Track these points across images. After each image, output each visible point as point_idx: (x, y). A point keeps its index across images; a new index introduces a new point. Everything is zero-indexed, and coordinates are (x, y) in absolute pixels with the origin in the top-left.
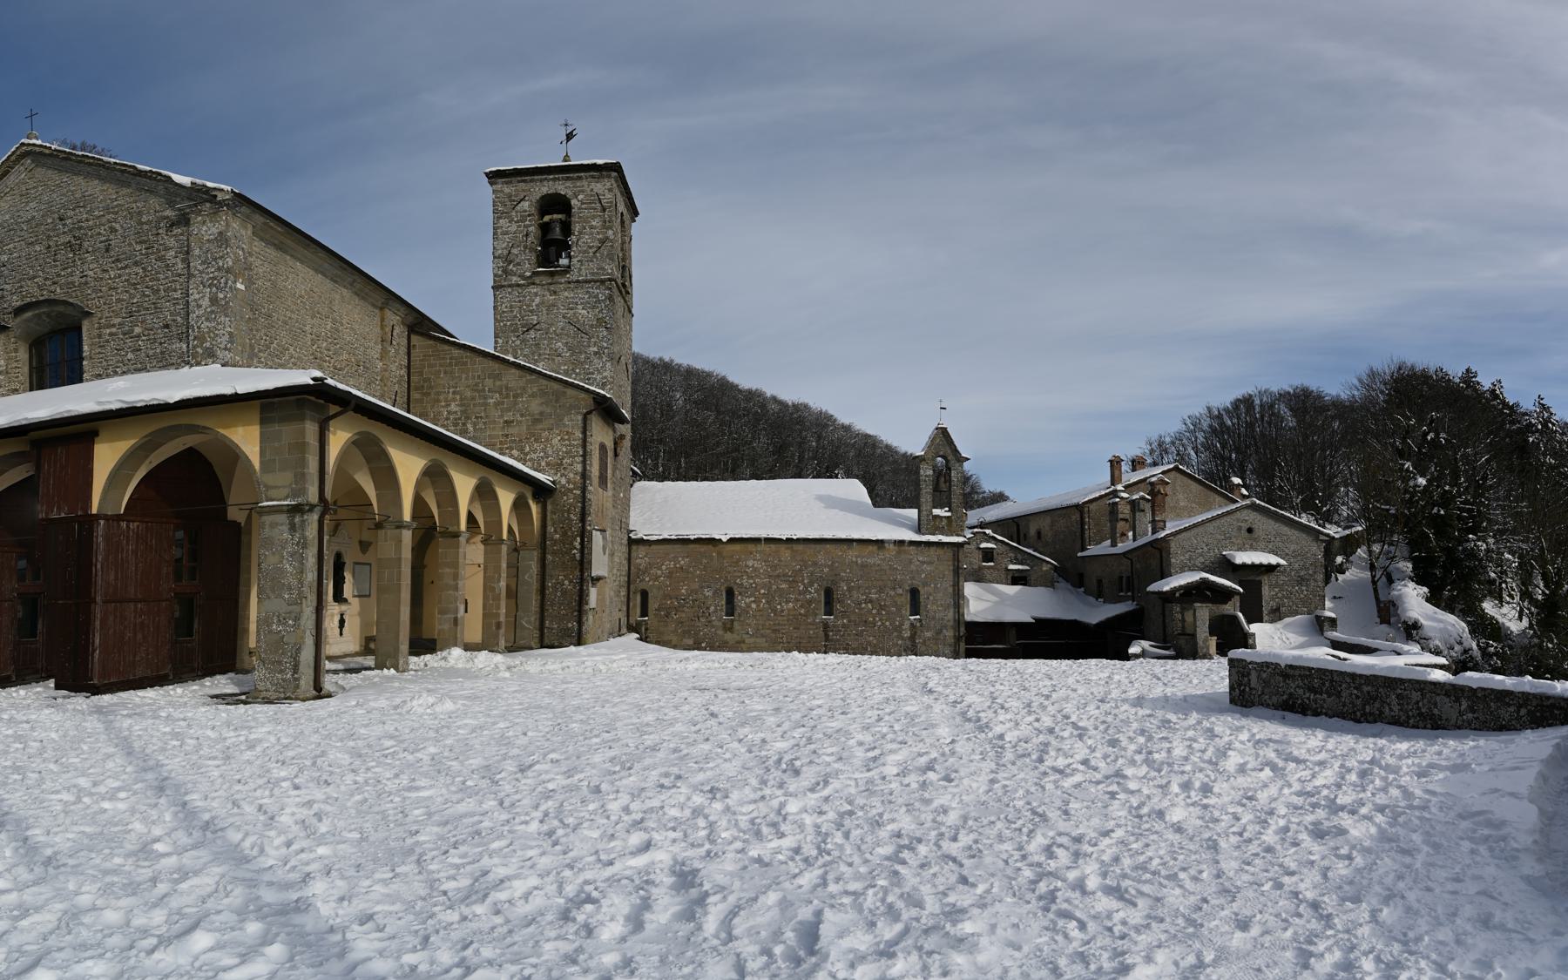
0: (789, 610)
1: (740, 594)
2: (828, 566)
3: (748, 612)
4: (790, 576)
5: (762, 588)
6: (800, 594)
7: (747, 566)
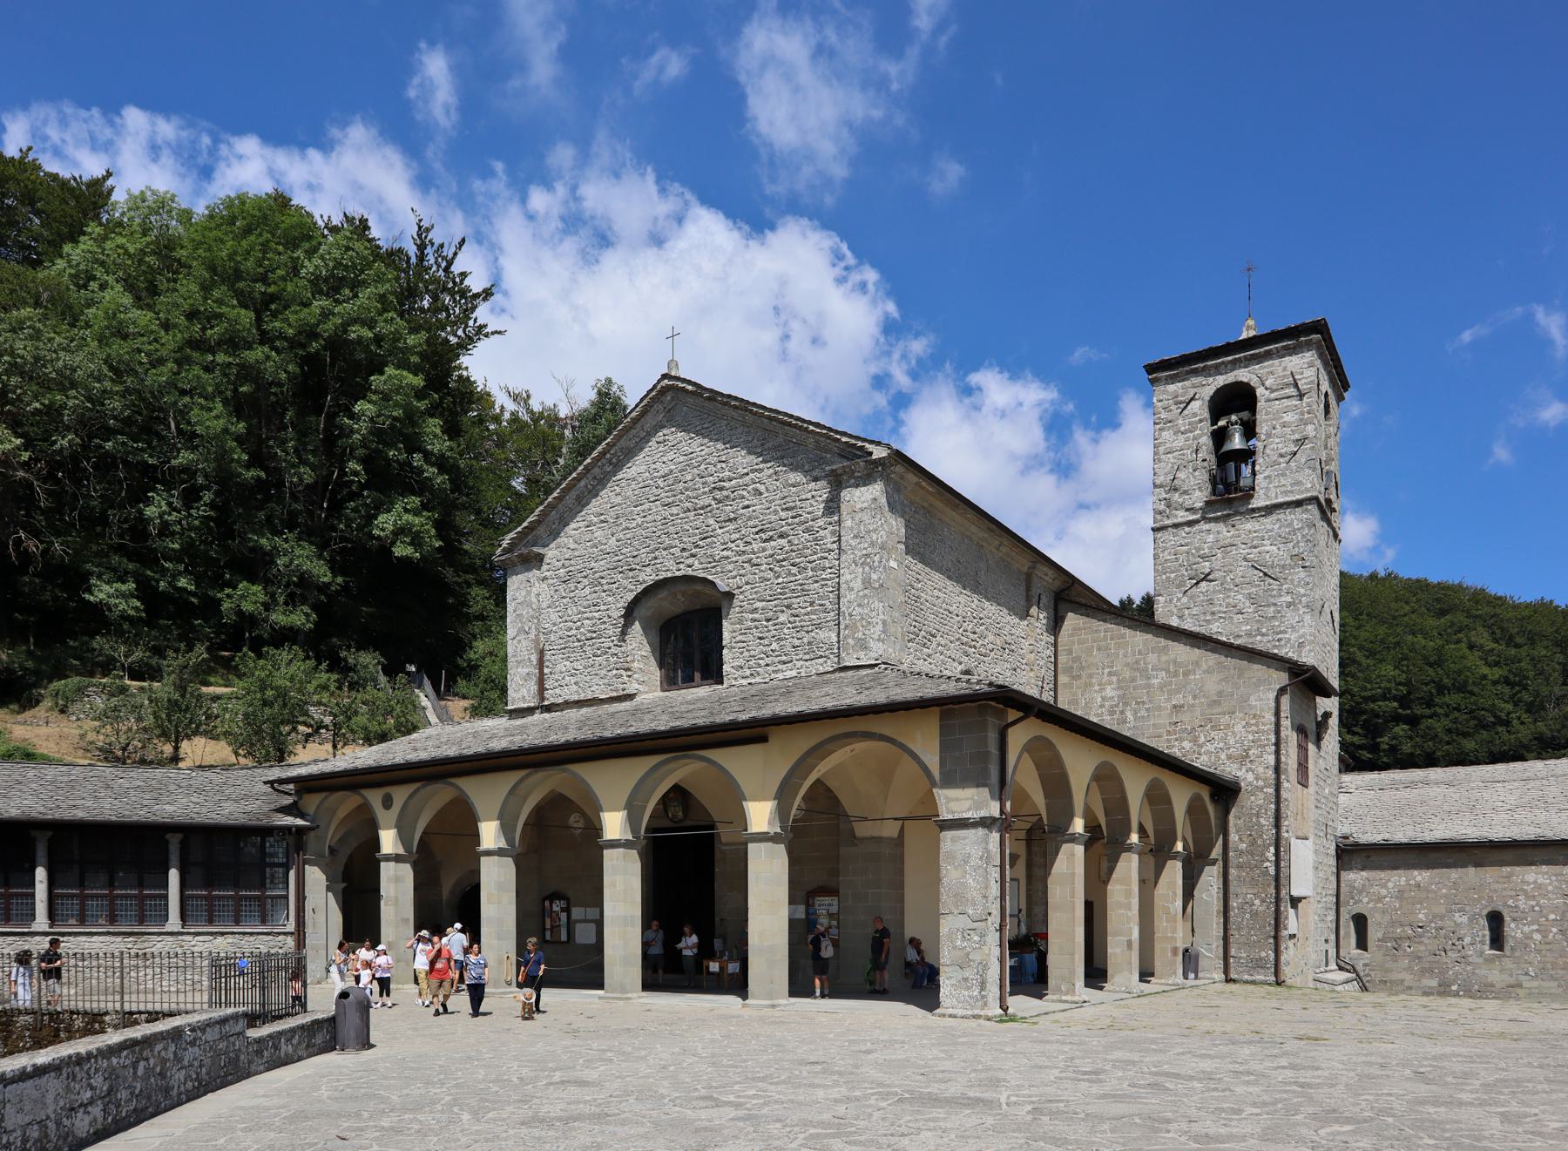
1: (1514, 920)
3: (1526, 946)
5: (1553, 912)
7: (1528, 883)
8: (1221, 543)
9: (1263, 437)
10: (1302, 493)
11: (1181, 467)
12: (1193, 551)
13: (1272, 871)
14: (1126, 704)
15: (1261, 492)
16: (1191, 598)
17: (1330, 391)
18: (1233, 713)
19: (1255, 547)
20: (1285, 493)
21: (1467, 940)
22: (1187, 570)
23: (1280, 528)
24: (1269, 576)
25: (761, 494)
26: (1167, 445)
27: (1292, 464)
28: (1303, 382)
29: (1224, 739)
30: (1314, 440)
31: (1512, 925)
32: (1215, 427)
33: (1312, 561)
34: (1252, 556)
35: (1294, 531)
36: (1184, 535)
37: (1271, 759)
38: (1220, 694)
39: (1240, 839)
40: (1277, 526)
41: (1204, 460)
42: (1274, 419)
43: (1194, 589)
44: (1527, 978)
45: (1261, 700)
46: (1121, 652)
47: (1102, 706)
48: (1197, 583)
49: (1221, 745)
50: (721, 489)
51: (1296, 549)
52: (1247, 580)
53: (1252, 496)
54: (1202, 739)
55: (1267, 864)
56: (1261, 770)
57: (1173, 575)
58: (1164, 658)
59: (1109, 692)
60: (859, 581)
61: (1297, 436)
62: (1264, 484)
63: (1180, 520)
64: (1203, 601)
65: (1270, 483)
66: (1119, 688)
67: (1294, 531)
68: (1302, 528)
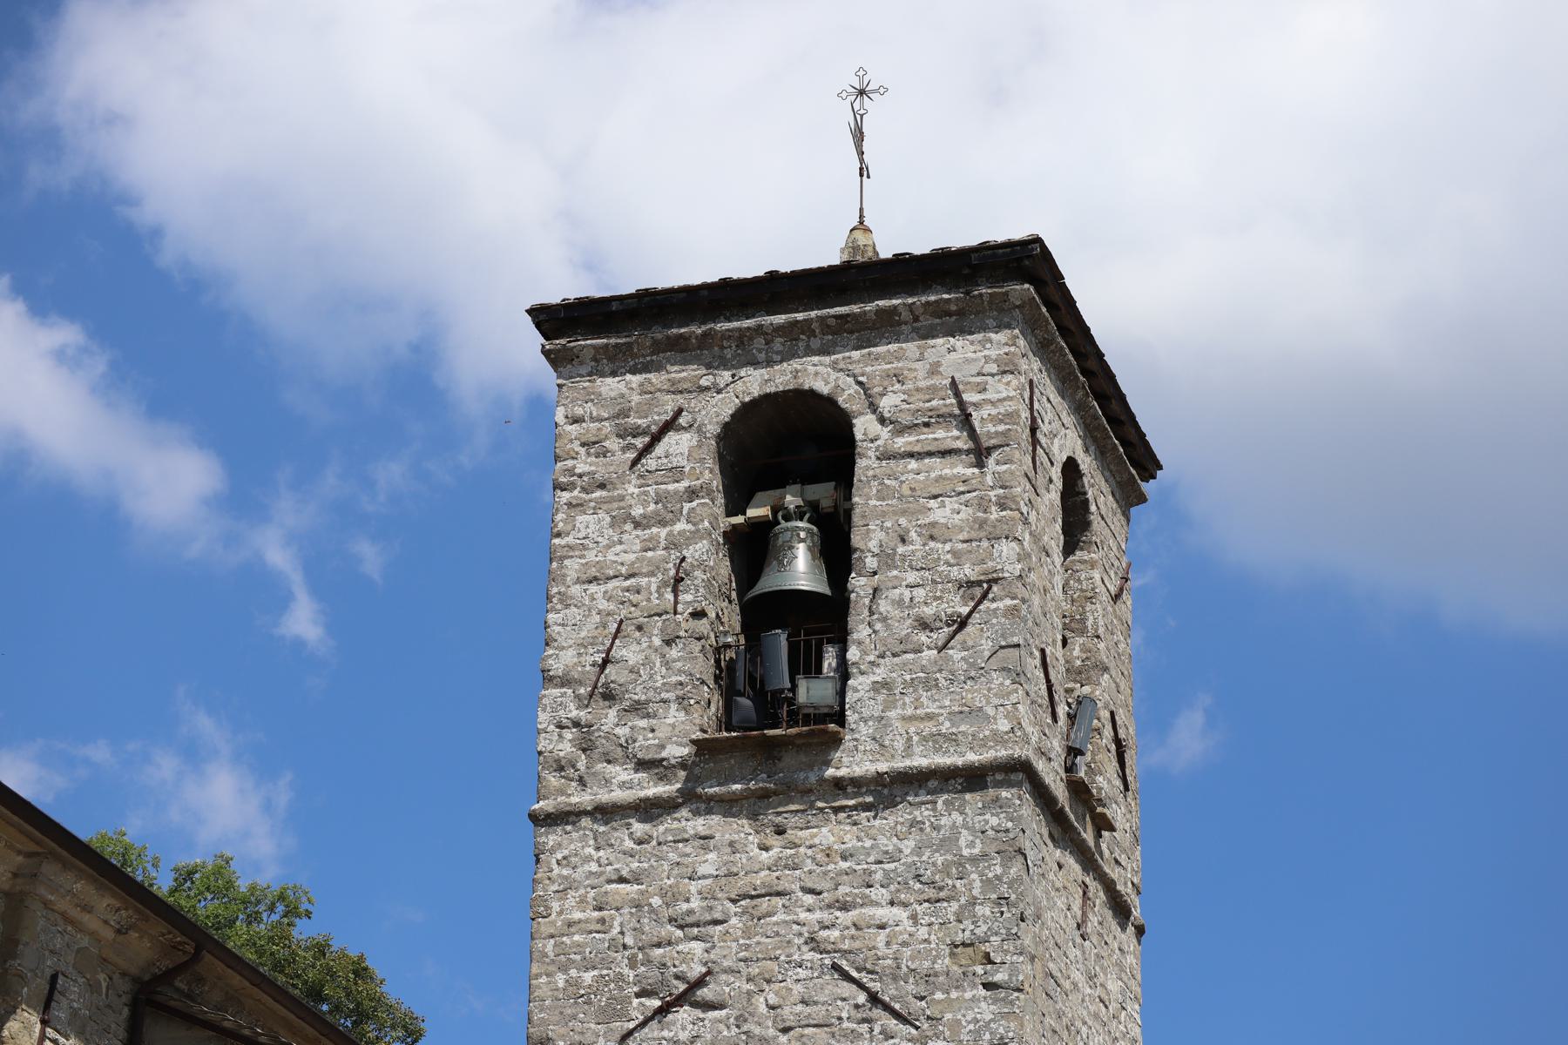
8: (742, 884)
9: (871, 563)
10: (984, 744)
11: (629, 628)
12: (656, 901)
15: (865, 731)
19: (845, 907)
20: (937, 740)
22: (633, 964)
23: (918, 850)
24: (887, 1008)
26: (591, 556)
27: (955, 654)
28: (985, 413)
30: (1021, 591)
32: (739, 519)
33: (1014, 970)
34: (834, 934)
35: (960, 866)
36: (629, 844)
40: (908, 845)
41: (698, 614)
42: (904, 512)
43: (652, 1030)
48: (663, 1011)
51: (967, 924)
52: (818, 1012)
53: (836, 741)
57: (588, 977)
61: (969, 571)
62: (873, 708)
63: (619, 796)
65: (889, 706)
67: (960, 866)
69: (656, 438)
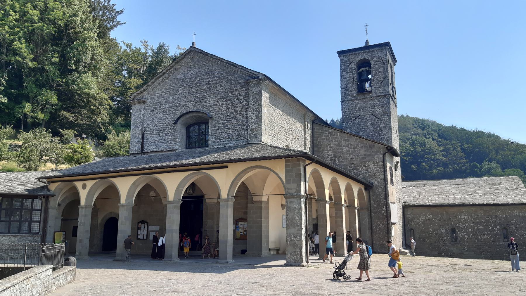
0: (485, 239)
1: (459, 231)
2: (504, 218)
3: (464, 240)
4: (484, 223)
6: (490, 231)
7: (462, 219)
13: (385, 214)
14: (336, 157)
16: (354, 123)
17: (392, 62)
18: (370, 161)
20: (381, 93)
21: (445, 238)
22: (352, 115)
23: (380, 103)
25: (222, 86)
28: (384, 60)
29: (367, 170)
31: (459, 233)
37: (383, 177)
38: (365, 155)
39: (374, 203)
40: (379, 103)
43: (354, 121)
44: (465, 251)
45: (378, 157)
46: (334, 140)
47: (328, 158)
49: (366, 171)
50: (210, 84)
54: (360, 170)
55: (383, 212)
56: (379, 180)
58: (347, 143)
59: (330, 153)
60: (255, 116)
64: (357, 125)
65: (376, 89)
66: (333, 152)
68: (386, 103)
69: (350, 64)
